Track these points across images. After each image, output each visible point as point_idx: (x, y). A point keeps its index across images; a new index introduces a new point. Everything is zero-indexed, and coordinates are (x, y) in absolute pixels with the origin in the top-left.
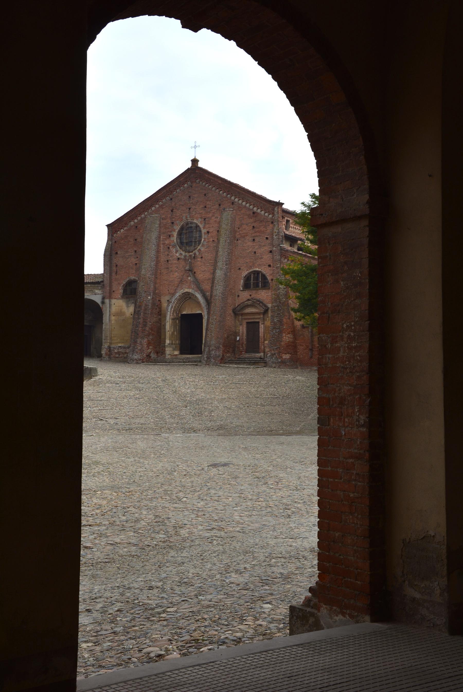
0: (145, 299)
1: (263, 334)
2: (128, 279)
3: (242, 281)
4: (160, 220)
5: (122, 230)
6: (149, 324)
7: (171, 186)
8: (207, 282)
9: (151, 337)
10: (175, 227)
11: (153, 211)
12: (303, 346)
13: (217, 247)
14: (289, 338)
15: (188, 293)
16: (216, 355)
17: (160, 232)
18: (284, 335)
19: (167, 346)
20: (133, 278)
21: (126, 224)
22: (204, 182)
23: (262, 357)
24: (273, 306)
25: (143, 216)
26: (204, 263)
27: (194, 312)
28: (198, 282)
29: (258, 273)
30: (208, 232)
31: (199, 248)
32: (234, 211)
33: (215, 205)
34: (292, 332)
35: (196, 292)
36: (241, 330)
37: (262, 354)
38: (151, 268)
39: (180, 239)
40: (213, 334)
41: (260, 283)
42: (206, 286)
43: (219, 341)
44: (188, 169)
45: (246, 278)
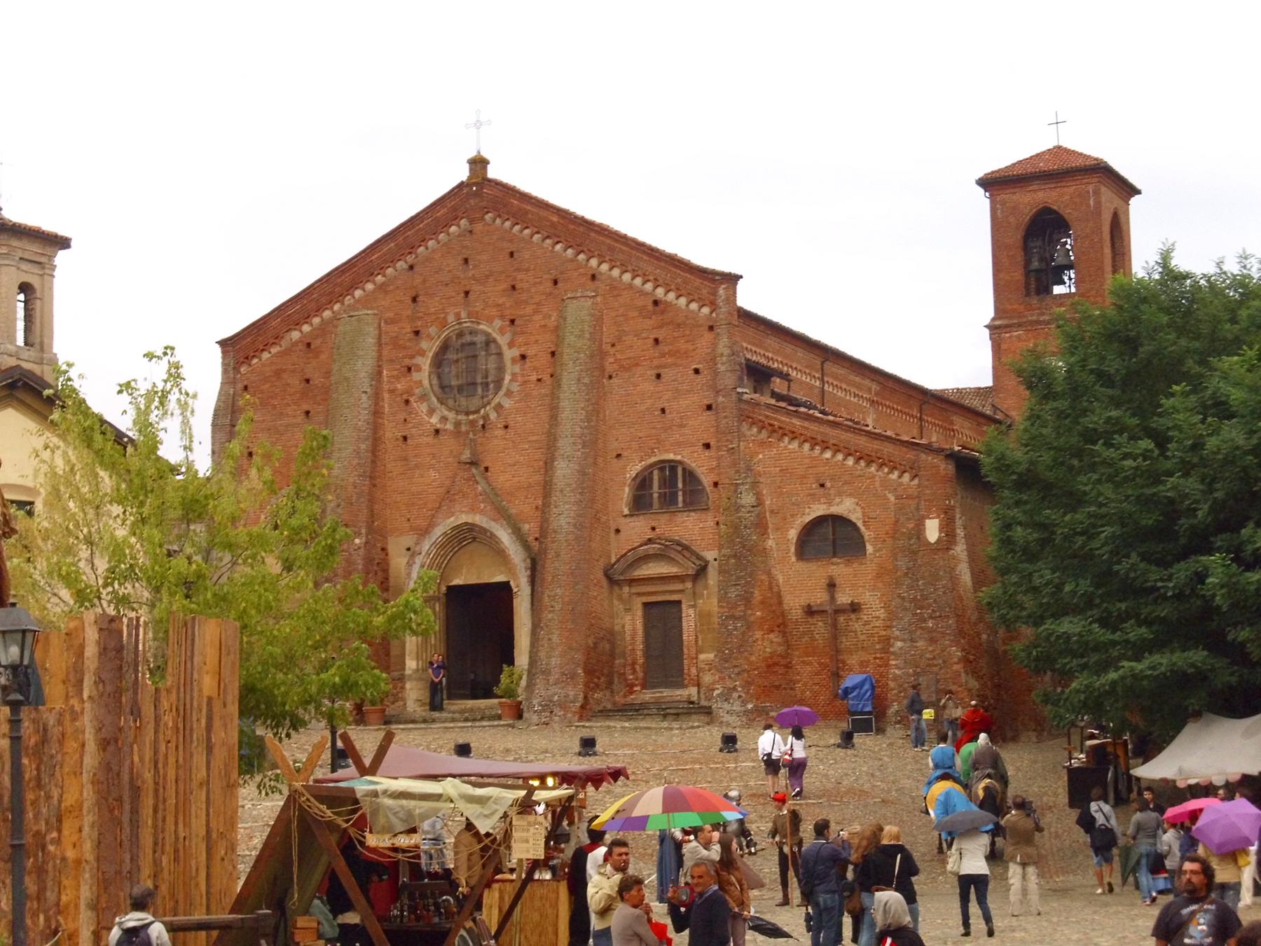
1: (692, 634)
3: (627, 489)
4: (380, 325)
5: (265, 355)
7: (410, 230)
10: (424, 345)
11: (358, 301)
12: (809, 664)
13: (554, 396)
15: (471, 528)
16: (567, 696)
17: (380, 358)
18: (758, 634)
19: (410, 675)
21: (278, 338)
22: (508, 219)
23: (692, 699)
24: (724, 556)
25: (327, 314)
26: (513, 442)
27: (486, 579)
28: (496, 495)
29: (673, 466)
30: (523, 357)
31: (496, 400)
32: (599, 299)
33: (540, 283)
34: (778, 626)
35: (493, 523)
36: (627, 627)
37: (693, 691)
38: (360, 458)
39: (439, 377)
40: (555, 638)
41: (680, 493)
42: (523, 506)
43: (573, 658)
44: (461, 185)
45: (638, 480)
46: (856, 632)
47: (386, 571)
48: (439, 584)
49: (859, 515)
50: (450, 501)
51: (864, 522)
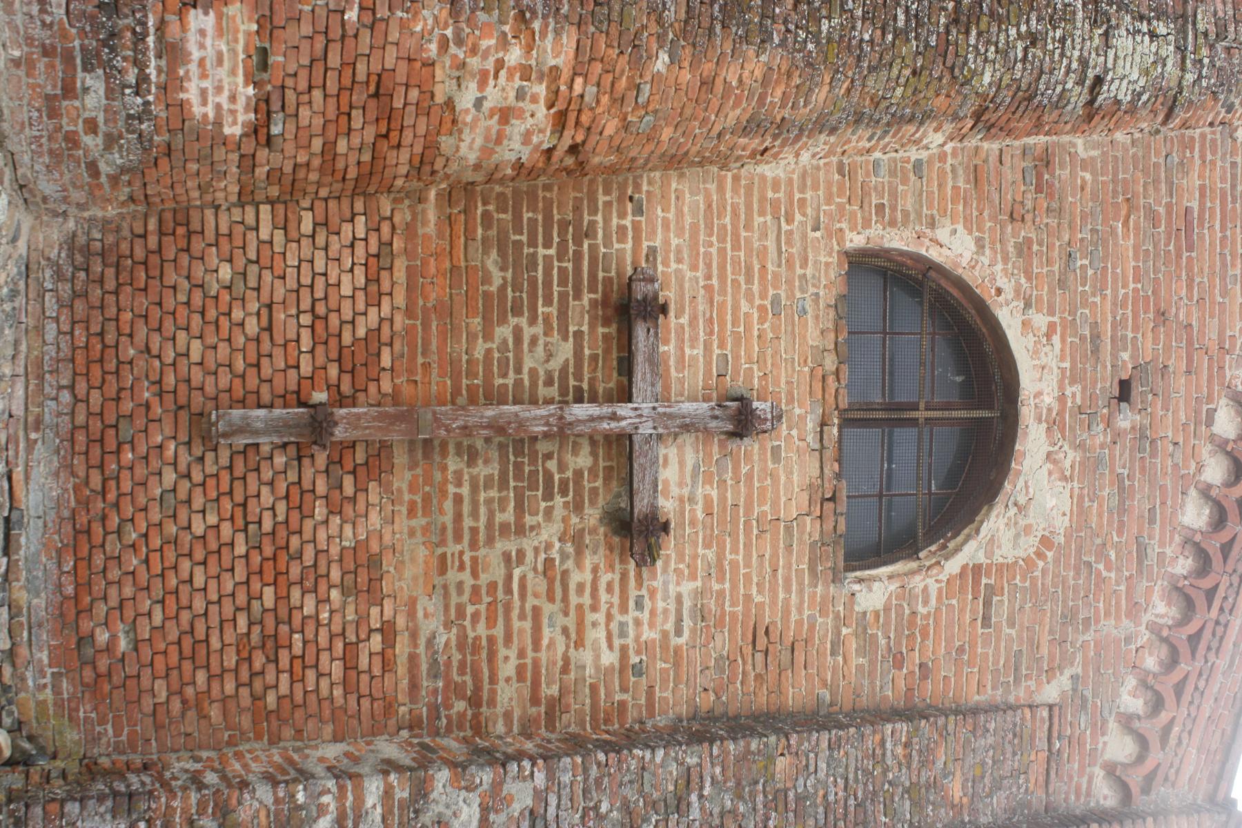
12: (373, 292)
14: (505, 115)
34: (574, 149)
46: (521, 530)
49: (1006, 552)
51: (977, 569)
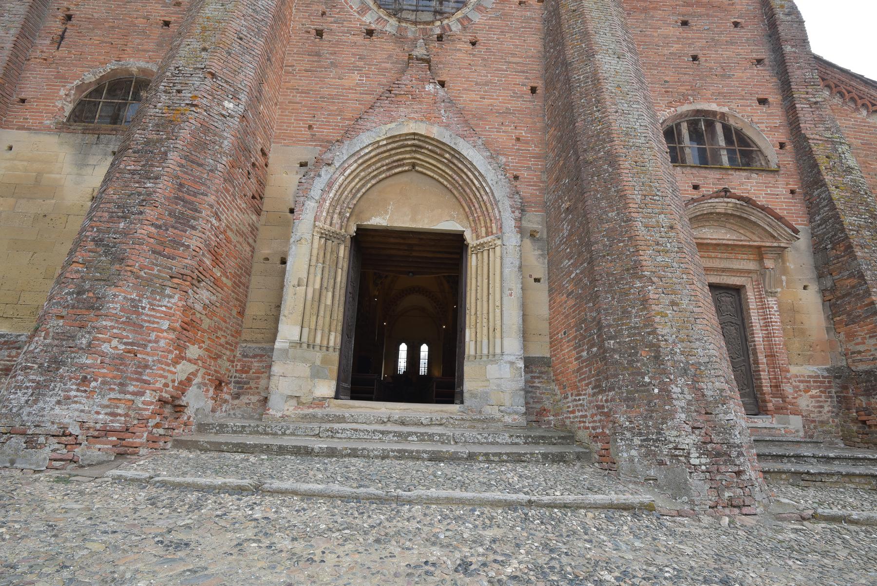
0: (204, 101)
2: (109, 67)
6: (205, 222)
8: (501, 120)
9: (205, 295)
15: (419, 142)
19: (285, 352)
20: (142, 64)
26: (484, 59)
29: (709, 118)
31: (459, 15)
35: (460, 141)
47: (261, 184)
48: (349, 218)
50: (392, 102)
